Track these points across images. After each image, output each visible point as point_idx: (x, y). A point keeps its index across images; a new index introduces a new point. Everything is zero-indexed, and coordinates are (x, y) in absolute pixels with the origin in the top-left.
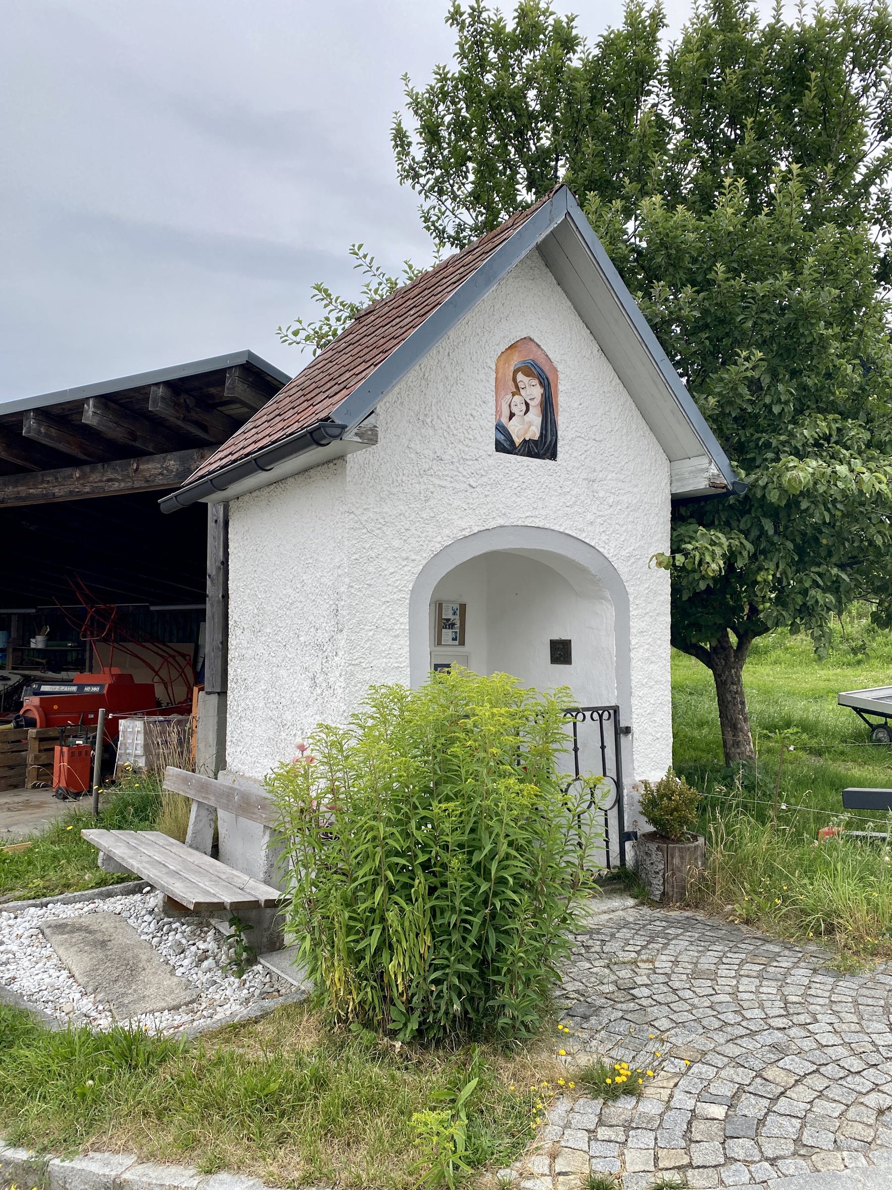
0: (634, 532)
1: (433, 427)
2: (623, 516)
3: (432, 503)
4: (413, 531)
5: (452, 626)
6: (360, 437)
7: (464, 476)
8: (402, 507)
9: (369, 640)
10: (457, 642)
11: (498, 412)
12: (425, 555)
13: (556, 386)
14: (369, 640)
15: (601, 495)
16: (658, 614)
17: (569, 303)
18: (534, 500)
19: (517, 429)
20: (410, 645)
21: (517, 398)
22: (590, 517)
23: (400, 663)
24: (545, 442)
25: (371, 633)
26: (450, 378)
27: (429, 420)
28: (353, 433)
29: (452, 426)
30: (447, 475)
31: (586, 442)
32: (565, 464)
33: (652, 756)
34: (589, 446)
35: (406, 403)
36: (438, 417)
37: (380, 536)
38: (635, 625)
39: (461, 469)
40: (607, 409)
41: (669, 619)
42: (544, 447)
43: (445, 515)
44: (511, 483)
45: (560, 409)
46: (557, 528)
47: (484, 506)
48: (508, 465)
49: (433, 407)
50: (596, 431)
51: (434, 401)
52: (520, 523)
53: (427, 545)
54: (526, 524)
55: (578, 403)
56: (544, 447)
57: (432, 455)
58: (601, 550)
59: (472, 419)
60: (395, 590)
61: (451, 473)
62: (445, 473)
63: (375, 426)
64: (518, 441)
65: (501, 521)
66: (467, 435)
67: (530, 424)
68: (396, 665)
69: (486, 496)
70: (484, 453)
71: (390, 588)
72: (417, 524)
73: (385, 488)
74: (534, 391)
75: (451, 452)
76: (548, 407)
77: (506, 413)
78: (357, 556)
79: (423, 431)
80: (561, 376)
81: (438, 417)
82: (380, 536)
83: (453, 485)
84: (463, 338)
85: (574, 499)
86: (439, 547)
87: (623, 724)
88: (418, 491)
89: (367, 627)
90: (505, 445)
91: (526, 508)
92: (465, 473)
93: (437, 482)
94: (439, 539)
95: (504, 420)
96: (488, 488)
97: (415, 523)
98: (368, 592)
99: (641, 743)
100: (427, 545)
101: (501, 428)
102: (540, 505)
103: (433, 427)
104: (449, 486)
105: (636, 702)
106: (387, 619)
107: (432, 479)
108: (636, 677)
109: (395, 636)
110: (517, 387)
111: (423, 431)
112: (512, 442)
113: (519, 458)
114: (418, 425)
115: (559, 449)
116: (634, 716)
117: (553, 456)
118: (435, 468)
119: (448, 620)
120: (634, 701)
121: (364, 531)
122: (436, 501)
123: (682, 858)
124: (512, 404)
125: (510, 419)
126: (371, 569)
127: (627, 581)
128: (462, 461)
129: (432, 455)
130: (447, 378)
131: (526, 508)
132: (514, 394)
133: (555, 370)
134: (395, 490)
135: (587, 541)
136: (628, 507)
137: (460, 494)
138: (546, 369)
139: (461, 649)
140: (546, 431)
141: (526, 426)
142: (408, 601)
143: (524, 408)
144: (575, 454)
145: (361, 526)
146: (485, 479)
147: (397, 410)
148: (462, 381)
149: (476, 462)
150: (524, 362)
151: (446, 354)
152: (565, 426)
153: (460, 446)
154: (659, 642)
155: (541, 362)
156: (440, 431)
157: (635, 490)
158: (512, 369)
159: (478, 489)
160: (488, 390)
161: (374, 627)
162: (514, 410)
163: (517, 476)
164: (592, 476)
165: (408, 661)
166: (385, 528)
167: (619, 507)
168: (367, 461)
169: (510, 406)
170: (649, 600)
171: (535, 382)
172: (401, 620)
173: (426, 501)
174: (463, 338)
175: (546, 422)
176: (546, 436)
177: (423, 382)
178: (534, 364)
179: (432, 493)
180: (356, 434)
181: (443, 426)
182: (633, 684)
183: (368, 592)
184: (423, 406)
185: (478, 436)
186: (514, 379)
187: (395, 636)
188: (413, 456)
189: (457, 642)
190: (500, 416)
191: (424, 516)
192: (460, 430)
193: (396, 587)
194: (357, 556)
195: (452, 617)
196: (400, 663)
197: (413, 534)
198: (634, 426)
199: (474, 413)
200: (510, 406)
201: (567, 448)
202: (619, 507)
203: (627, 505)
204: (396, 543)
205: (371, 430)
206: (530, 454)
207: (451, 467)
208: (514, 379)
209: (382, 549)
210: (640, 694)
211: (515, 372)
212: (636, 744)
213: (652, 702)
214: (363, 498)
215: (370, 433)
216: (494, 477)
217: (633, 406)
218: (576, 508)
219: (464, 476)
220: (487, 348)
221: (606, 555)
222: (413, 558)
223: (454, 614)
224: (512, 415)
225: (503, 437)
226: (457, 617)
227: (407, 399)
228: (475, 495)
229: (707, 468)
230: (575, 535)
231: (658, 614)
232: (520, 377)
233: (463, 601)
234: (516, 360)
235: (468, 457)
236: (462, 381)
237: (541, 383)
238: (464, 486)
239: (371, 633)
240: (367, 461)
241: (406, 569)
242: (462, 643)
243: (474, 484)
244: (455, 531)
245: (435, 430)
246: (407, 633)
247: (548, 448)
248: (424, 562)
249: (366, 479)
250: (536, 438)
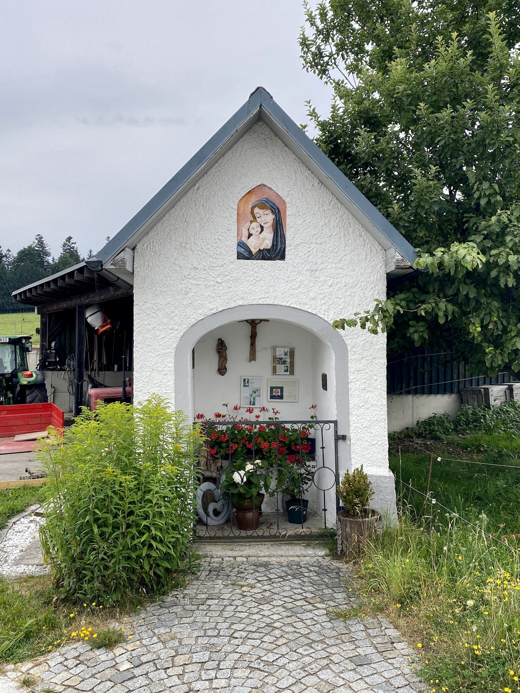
0: (351, 302)
1: (191, 250)
2: (341, 292)
3: (190, 295)
4: (177, 313)
5: (284, 362)
6: (114, 266)
7: (213, 277)
8: (170, 299)
9: (147, 377)
10: (288, 373)
11: (239, 233)
12: (184, 326)
13: (285, 212)
14: (147, 377)
15: (322, 280)
16: (374, 358)
17: (294, 157)
18: (266, 287)
19: (254, 243)
20: (175, 380)
21: (254, 224)
22: (312, 295)
23: (168, 390)
24: (276, 250)
25: (149, 373)
26: (203, 219)
27: (188, 246)
28: (110, 264)
29: (204, 248)
30: (201, 278)
31: (308, 246)
32: (292, 262)
33: (368, 456)
34: (311, 249)
35: (173, 238)
36: (195, 244)
37: (155, 316)
38: (352, 366)
39: (210, 273)
40: (327, 221)
41: (385, 361)
42: (276, 252)
43: (199, 302)
44: (248, 278)
45: (287, 227)
46: (284, 304)
47: (227, 294)
48: (246, 267)
49: (192, 238)
50: (318, 237)
51: (193, 234)
52: (255, 302)
53: (186, 320)
54: (259, 303)
55: (301, 221)
56: (276, 252)
57: (190, 267)
58: (322, 316)
59: (219, 241)
60: (164, 348)
61: (203, 276)
62: (199, 276)
63: (124, 258)
64: (254, 251)
65: (240, 303)
66: (215, 252)
67: (264, 239)
68: (165, 391)
69: (229, 288)
70: (228, 261)
71: (161, 347)
72: (180, 308)
73: (159, 289)
74: (267, 218)
75: (204, 263)
76: (278, 228)
77: (245, 234)
78: (140, 329)
79: (184, 253)
80: (288, 205)
81: (195, 244)
82: (155, 316)
83: (205, 283)
84: (213, 193)
85: (298, 284)
86: (194, 321)
87: (340, 433)
88: (180, 289)
89: (146, 370)
90: (245, 254)
91: (260, 293)
92: (213, 275)
93: (194, 282)
94: (195, 316)
95: (244, 239)
96: (231, 282)
97: (178, 308)
98: (147, 349)
99: (357, 447)
100: (186, 320)
101: (241, 244)
102: (271, 289)
103: (191, 250)
104: (202, 284)
105: (354, 419)
106: (159, 365)
107: (191, 281)
108: (353, 402)
109: (165, 375)
110: (254, 217)
111: (184, 253)
112: (250, 252)
113: (255, 262)
114: (181, 250)
115: (286, 253)
116: (352, 428)
117: (282, 257)
118: (192, 274)
119: (281, 359)
120: (352, 418)
121: (145, 314)
122: (192, 294)
123: (351, 528)
124: (250, 228)
125: (249, 237)
126: (148, 336)
127: (345, 336)
128: (211, 268)
129: (190, 267)
130: (202, 219)
131: (260, 293)
132: (251, 222)
133: (284, 202)
134: (164, 290)
135: (310, 311)
136: (345, 286)
137: (210, 288)
138: (277, 202)
139: (291, 377)
140: (277, 242)
141: (261, 241)
142: (173, 354)
143: (259, 229)
144: (300, 255)
145: (143, 312)
146: (229, 277)
147: (167, 243)
148: (212, 220)
149: (222, 267)
150: (259, 201)
151: (201, 204)
152: (291, 237)
153: (211, 259)
154: (375, 377)
155: (273, 198)
156: (196, 252)
157: (353, 273)
158: (250, 206)
159: (223, 284)
160: (231, 222)
161: (150, 370)
162: (252, 232)
163: (253, 273)
164: (314, 268)
165: (173, 389)
166: (158, 312)
167: (338, 286)
168: (146, 275)
169: (248, 230)
170: (366, 348)
171: (269, 212)
172: (169, 365)
173: (186, 294)
174: (213, 193)
175: (277, 236)
176: (277, 245)
177: (186, 223)
178: (268, 201)
179: (190, 289)
180: (112, 264)
181: (198, 248)
182: (351, 406)
183: (147, 349)
184: (185, 238)
185: (223, 252)
186: (252, 213)
187: (165, 375)
188: (177, 268)
189: (288, 373)
190: (241, 237)
191: (184, 303)
192: (210, 250)
193: (165, 346)
194: (140, 329)
195: (284, 357)
196: (168, 390)
197: (177, 314)
198: (351, 230)
199: (221, 238)
200: (248, 230)
201: (293, 251)
202: (338, 286)
203: (344, 284)
204: (165, 320)
205: (121, 261)
206: (264, 258)
207: (204, 272)
208: (252, 213)
209: (156, 324)
210: (357, 414)
211: (253, 208)
212: (353, 448)
213: (368, 419)
214: (144, 296)
215: (120, 262)
216: (235, 276)
217: (350, 216)
218: (301, 290)
219: (213, 277)
220: (231, 196)
221: (326, 320)
222: (176, 328)
223: (286, 354)
224: (250, 235)
225: (243, 250)
226: (288, 357)
227: (174, 236)
228: (221, 288)
229: (399, 255)
230: (299, 307)
231: (374, 358)
232: (257, 210)
233: (292, 346)
234: (253, 200)
235: (216, 265)
236: (212, 220)
237: (273, 212)
238: (212, 283)
239: (149, 373)
240: (146, 275)
241: (171, 335)
242: (292, 373)
243: (219, 281)
244: (206, 311)
245: (193, 251)
246: (173, 372)
247: (279, 253)
248: (184, 331)
249: (146, 285)
250: (269, 247)
